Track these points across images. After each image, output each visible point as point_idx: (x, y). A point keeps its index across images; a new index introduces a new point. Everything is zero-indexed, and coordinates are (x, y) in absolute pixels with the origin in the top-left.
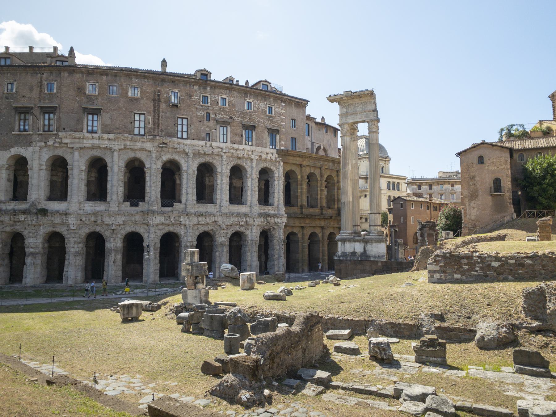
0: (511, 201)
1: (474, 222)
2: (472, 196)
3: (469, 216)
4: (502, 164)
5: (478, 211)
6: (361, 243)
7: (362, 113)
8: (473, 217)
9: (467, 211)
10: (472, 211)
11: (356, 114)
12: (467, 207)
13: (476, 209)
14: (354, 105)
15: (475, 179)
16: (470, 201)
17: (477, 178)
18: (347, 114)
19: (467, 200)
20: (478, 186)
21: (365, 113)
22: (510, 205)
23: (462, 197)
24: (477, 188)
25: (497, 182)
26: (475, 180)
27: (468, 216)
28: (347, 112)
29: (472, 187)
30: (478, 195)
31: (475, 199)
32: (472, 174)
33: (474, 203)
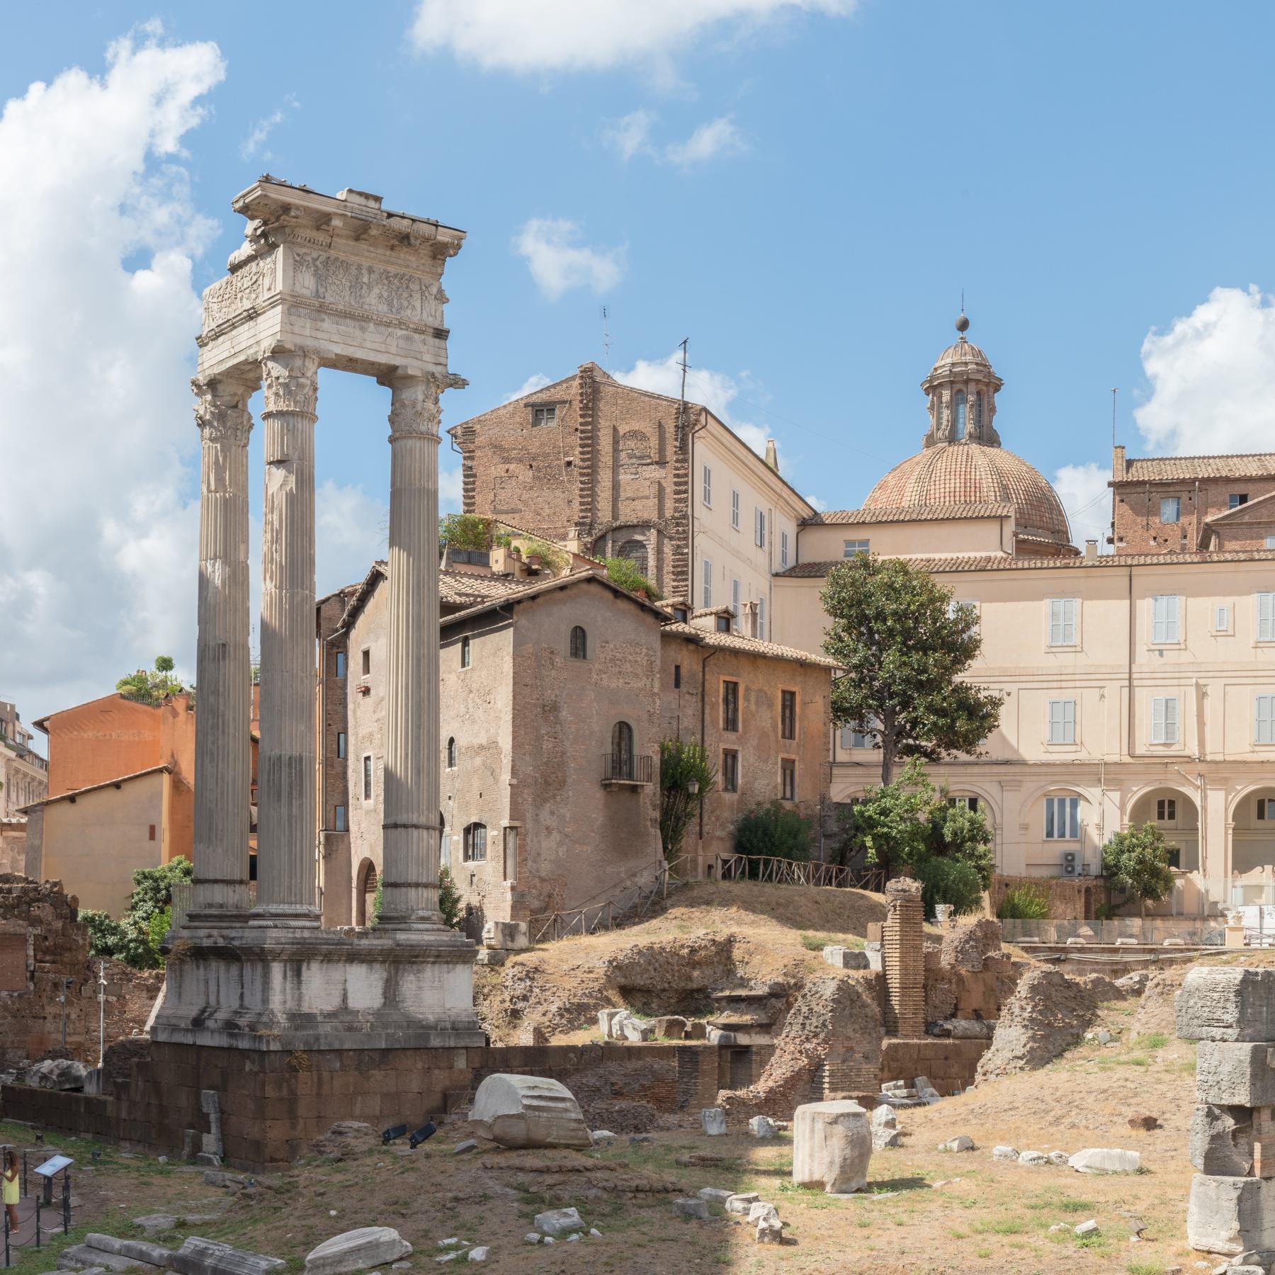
0: (657, 814)
1: (547, 888)
2: (547, 783)
3: (534, 861)
4: (639, 671)
5: (560, 844)
6: (377, 966)
7: (388, 325)
8: (545, 868)
9: (528, 840)
10: (544, 845)
11: (362, 319)
12: (530, 825)
13: (556, 836)
14: (354, 271)
15: (557, 717)
16: (540, 801)
17: (564, 713)
18: (322, 310)
19: (528, 796)
20: (567, 743)
21: (400, 333)
22: (652, 830)
23: (515, 782)
24: (563, 753)
25: (623, 731)
26: (558, 721)
27: (530, 863)
28: (317, 295)
29: (547, 745)
30: (562, 783)
31: (554, 796)
32: (550, 695)
33: (552, 813)
